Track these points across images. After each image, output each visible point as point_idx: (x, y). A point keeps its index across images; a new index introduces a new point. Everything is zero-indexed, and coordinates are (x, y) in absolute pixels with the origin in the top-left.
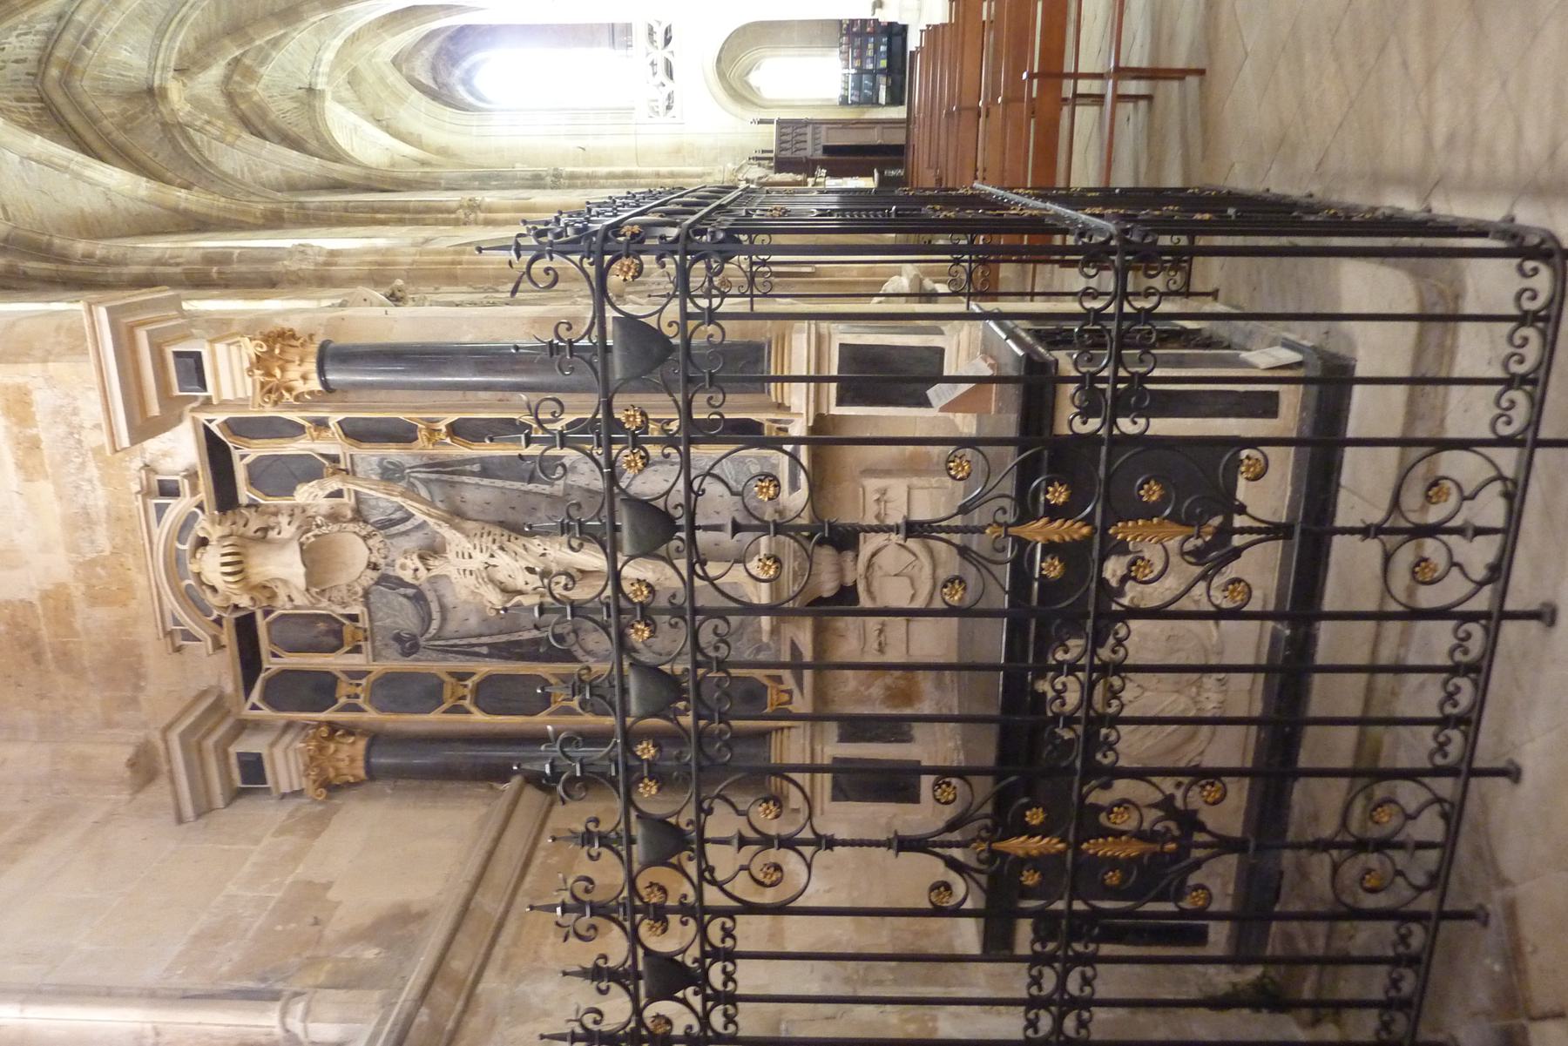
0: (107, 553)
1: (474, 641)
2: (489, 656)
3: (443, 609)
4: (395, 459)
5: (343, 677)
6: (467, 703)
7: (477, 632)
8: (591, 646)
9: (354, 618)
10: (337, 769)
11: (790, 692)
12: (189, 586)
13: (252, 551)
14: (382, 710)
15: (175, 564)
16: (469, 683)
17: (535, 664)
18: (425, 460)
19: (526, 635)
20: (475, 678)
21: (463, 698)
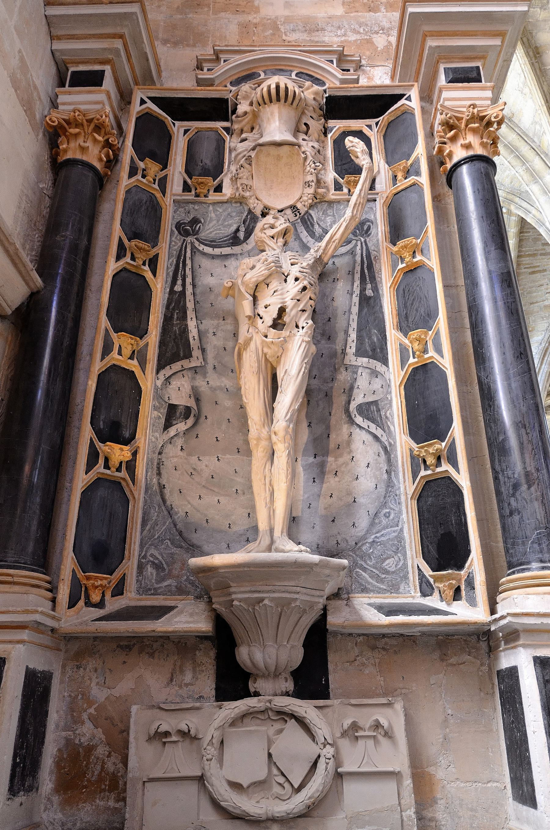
0: (284, 37)
1: (189, 280)
2: (172, 291)
3: (226, 257)
4: (373, 231)
6: (128, 259)
7: (199, 283)
8: (175, 383)
9: (219, 189)
10: (76, 135)
11: (101, 605)
12: (260, 76)
14: (128, 192)
15: (278, 66)
16: (147, 268)
17: (159, 329)
18: (373, 254)
19: (192, 324)
21: (133, 258)
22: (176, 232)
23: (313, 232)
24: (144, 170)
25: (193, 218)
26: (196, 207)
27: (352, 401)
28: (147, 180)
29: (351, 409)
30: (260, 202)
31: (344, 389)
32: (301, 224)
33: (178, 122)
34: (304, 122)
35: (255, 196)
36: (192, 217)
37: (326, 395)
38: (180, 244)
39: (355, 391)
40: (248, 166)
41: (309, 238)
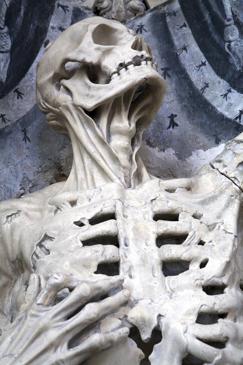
23: (221, 51)
32: (182, 19)
41: (210, 73)
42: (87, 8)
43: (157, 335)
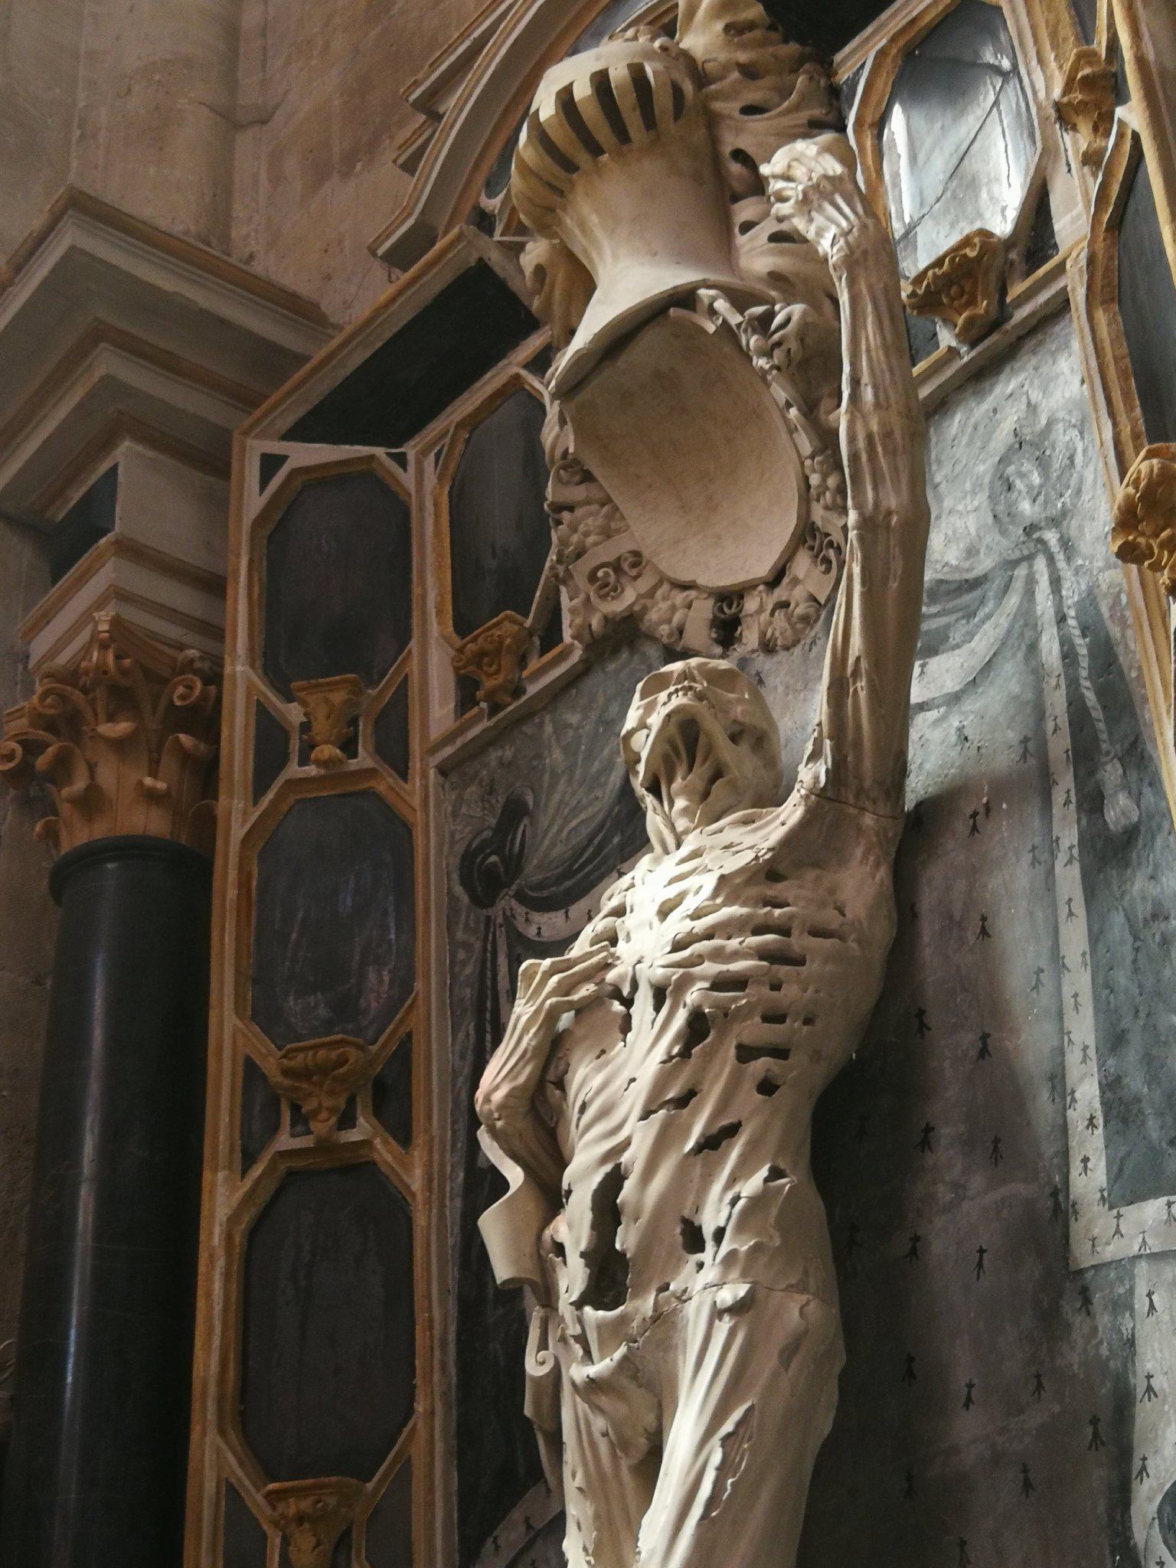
5: (378, 695)
13: (651, 168)
20: (385, 1151)
22: (465, 899)
24: (306, 727)
25: (505, 807)
26: (509, 753)
27: (1135, 1484)
28: (320, 763)
29: (1139, 1535)
30: (693, 594)
31: (1095, 1421)
33: (412, 443)
34: (727, 150)
35: (666, 587)
36: (502, 799)
37: (1027, 1486)
38: (478, 945)
39: (1144, 1411)
40: (578, 493)
42: (753, 651)
43: (635, 986)
